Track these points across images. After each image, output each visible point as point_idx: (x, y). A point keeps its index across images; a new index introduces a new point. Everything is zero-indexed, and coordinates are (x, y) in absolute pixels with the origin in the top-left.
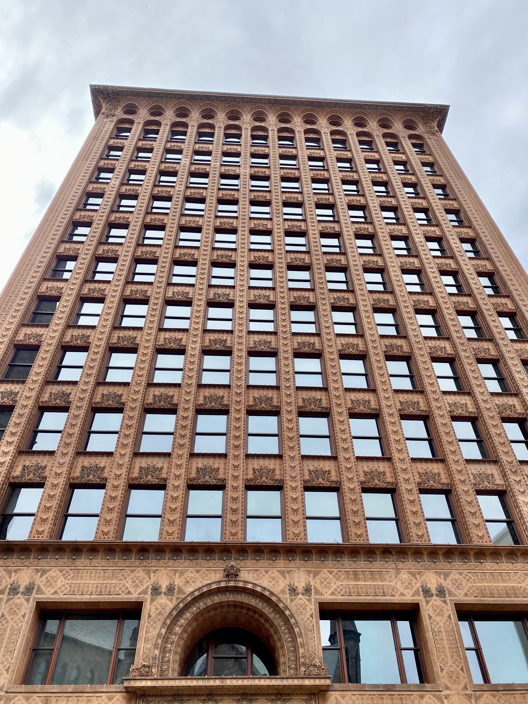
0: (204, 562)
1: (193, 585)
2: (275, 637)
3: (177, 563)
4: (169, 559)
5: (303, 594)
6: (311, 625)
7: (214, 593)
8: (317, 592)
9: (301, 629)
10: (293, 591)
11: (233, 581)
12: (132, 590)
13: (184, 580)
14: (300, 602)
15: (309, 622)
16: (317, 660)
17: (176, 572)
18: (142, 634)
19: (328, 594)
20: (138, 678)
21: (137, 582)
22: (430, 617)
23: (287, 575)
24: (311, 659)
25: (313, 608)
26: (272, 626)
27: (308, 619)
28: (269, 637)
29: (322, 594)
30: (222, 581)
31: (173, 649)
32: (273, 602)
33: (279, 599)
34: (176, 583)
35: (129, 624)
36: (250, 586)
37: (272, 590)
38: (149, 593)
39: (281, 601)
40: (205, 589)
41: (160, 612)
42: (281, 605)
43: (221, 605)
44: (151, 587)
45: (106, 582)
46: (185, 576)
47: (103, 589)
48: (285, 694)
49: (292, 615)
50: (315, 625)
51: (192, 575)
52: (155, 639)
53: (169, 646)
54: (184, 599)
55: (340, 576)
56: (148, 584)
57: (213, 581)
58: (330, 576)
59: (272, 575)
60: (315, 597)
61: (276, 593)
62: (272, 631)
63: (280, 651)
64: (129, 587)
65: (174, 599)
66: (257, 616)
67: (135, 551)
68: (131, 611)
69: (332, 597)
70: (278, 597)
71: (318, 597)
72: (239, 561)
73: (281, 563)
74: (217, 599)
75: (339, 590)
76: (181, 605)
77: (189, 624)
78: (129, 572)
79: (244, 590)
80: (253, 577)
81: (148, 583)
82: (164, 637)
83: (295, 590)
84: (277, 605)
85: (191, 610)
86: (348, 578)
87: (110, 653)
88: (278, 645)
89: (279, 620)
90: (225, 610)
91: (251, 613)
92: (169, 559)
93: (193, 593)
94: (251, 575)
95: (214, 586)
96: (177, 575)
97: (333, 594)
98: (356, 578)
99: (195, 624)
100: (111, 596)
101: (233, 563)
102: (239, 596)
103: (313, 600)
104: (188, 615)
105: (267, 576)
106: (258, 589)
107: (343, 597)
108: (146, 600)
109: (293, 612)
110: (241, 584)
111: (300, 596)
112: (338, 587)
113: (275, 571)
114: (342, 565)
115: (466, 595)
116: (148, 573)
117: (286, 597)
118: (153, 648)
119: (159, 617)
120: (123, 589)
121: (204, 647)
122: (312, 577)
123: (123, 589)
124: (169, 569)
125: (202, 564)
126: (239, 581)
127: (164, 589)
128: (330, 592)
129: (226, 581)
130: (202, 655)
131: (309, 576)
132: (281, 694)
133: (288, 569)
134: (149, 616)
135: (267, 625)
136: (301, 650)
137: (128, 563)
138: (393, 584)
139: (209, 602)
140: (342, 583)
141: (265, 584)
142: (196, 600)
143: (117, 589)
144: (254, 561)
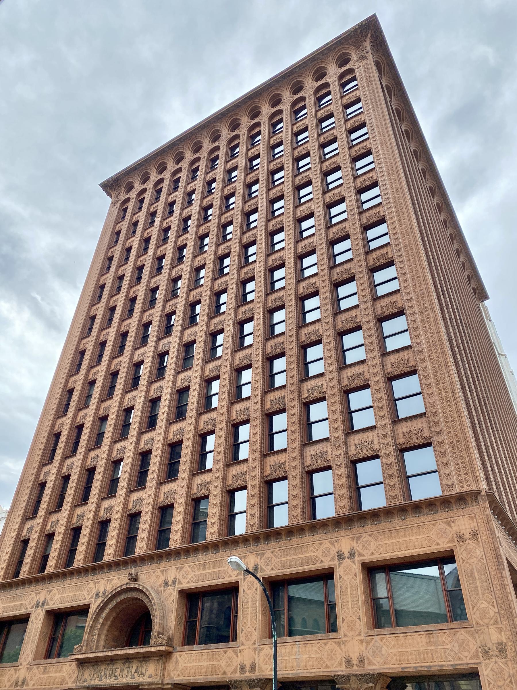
8: (180, 583)
12: (86, 597)
22: (244, 591)
29: (182, 584)
97: (188, 582)
98: (204, 568)
111: (170, 587)
115: (272, 569)
138: (226, 569)
139: (118, 600)
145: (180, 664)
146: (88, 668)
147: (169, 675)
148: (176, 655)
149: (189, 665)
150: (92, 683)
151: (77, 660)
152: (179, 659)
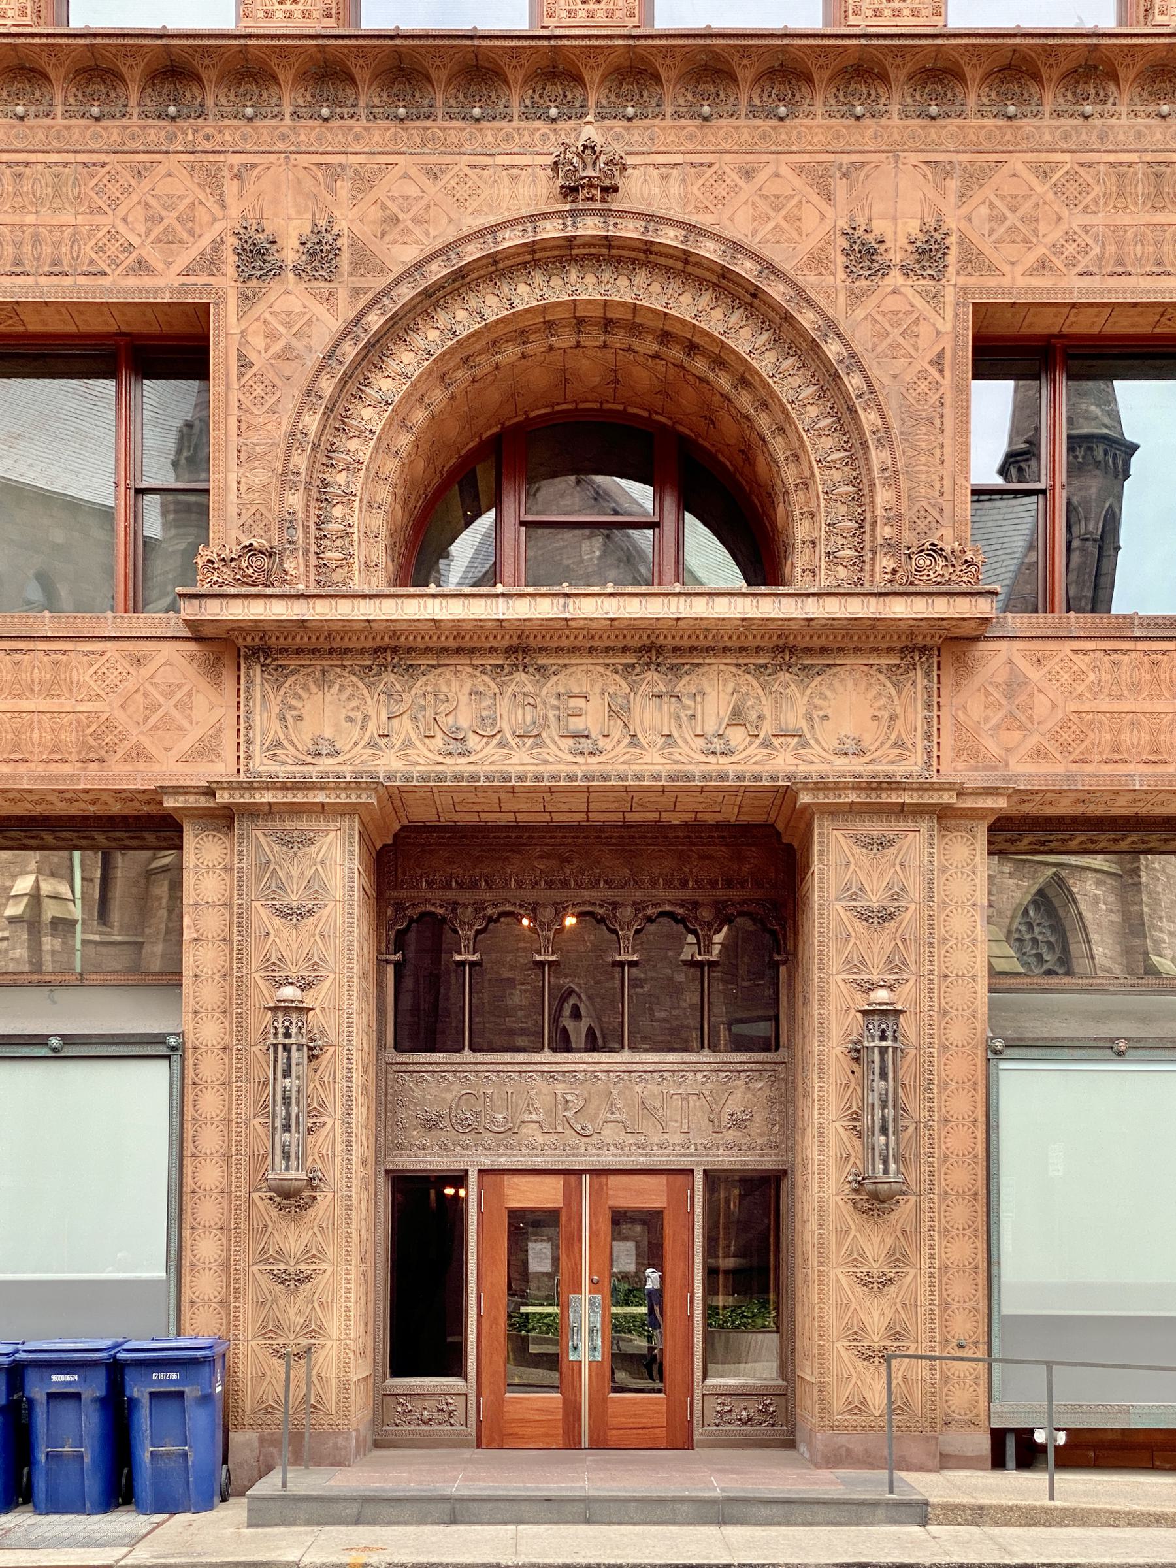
0: (457, 131)
1: (418, 231)
2: (778, 447)
3: (337, 133)
4: (296, 115)
5: (906, 271)
6: (934, 398)
7: (511, 269)
8: (972, 260)
9: (890, 414)
10: (864, 255)
11: (593, 212)
12: (154, 257)
13: (375, 213)
14: (891, 303)
15: (923, 386)
16: (947, 533)
17: (335, 174)
18: (224, 435)
19: (1019, 269)
20: (233, 591)
21: (170, 218)
23: (840, 187)
24: (922, 526)
25: (949, 330)
26: (765, 405)
27: (922, 374)
28: (749, 449)
29: (992, 269)
30: (545, 216)
31: (357, 489)
32: (774, 306)
33: (800, 292)
34: (341, 225)
35: (163, 399)
36: (670, 237)
37: (767, 252)
38: (231, 270)
39: (809, 301)
40: (473, 252)
41: (288, 347)
42: (807, 319)
43: (546, 320)
44: (233, 241)
45: (30, 219)
46: (379, 192)
47: (27, 249)
48: (807, 650)
49: (854, 360)
50: (948, 400)
51: (412, 190)
52: (281, 451)
53: (342, 478)
54: (386, 292)
55: (1086, 189)
56: (217, 228)
57: (506, 216)
58: (1039, 188)
59: (773, 188)
60: (961, 281)
61: (787, 267)
62: (763, 422)
63: (798, 500)
64: (136, 241)
65: (342, 295)
66: (699, 365)
67: (134, 73)
68: (166, 348)
69: (1036, 282)
70: (792, 283)
71: (972, 280)
72: (619, 125)
73: (817, 127)
74: (526, 294)
75: (1071, 249)
76: (376, 321)
77: (416, 396)
78: (126, 178)
79: (642, 257)
80: (685, 200)
81: (218, 227)
82: (315, 447)
83: (871, 253)
84: (788, 318)
85: (417, 340)
86: (1121, 194)
87: (106, 514)
88: (790, 474)
89: (795, 381)
90: (565, 339)
91: (676, 353)
92: (296, 115)
93: (418, 266)
94: (675, 188)
95: (511, 239)
96: (344, 188)
97: (1043, 266)
99: (438, 396)
100: (68, 281)
101: (590, 133)
102: (623, 282)
103: (950, 295)
104: (408, 361)
105: (747, 189)
106: (709, 250)
107: (1086, 282)
108: (221, 301)
109: (858, 349)
110: (630, 230)
111: (895, 278)
112: (1070, 237)
113: (784, 170)
114: (1101, 139)
116: (212, 179)
117: (830, 286)
118: (275, 484)
119: (287, 368)
120: (113, 249)
121: (482, 486)
122: (952, 199)
123: (113, 249)
124: (304, 160)
125: (453, 136)
126: (621, 214)
127: (291, 253)
128: (1031, 259)
129: (560, 214)
130: (478, 515)
131: (943, 193)
132: (793, 650)
133: (846, 159)
134: (245, 364)
135: (745, 401)
136: (883, 496)
137: (115, 137)
140: (1088, 219)
141: (740, 228)
142: (433, 299)
143: (88, 250)
144: (690, 124)
145: (1040, 699)
146: (323, 682)
147: (970, 750)
148: (995, 659)
149: (1105, 706)
150: (390, 763)
151: (199, 633)
152: (1035, 675)
